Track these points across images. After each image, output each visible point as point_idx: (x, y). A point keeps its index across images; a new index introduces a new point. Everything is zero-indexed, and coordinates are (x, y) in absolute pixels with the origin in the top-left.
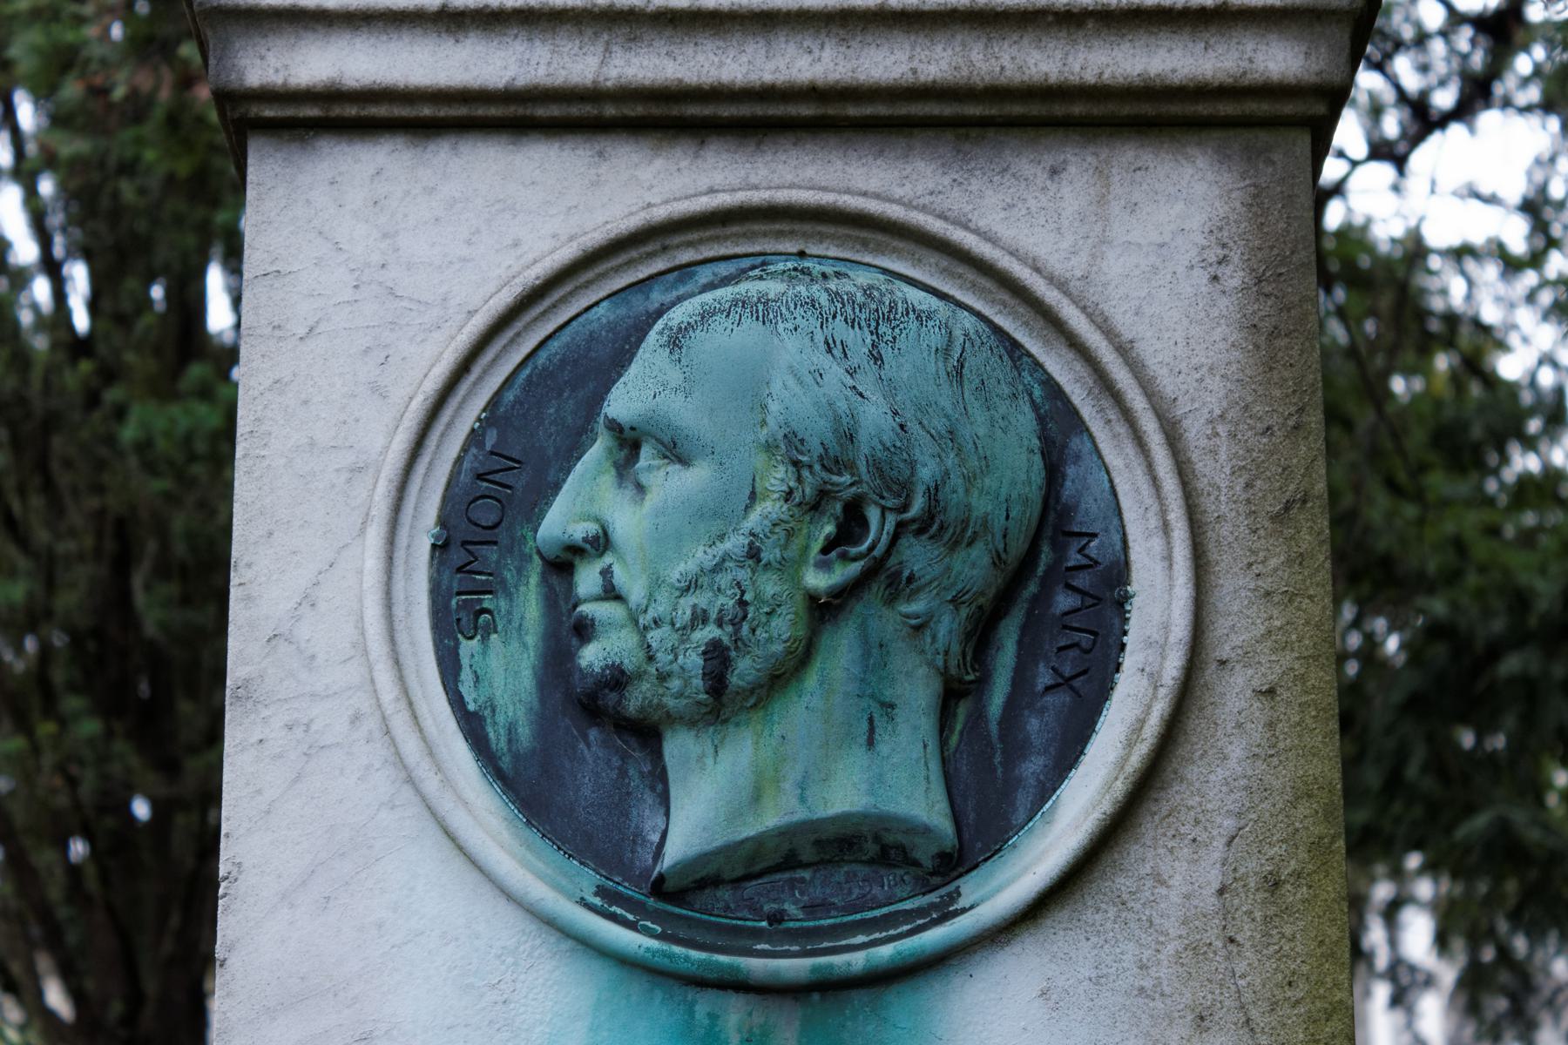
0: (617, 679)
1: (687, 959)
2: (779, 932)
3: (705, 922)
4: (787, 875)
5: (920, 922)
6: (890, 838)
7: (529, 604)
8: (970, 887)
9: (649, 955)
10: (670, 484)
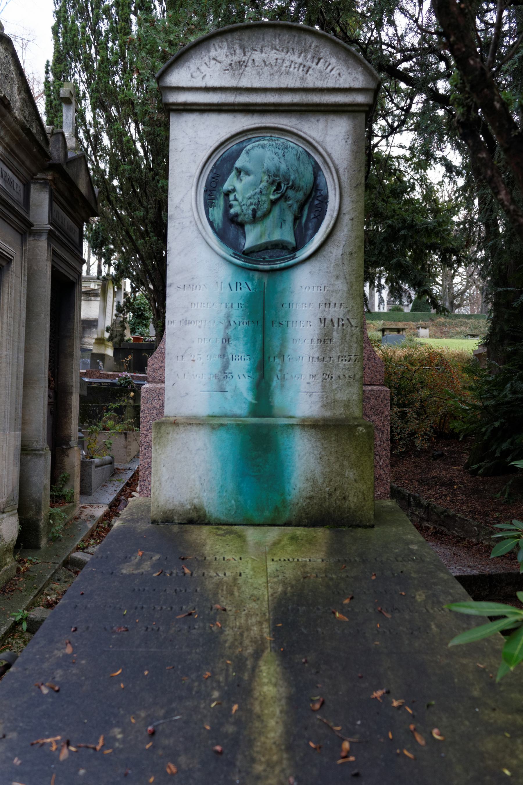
0: (237, 215)
2: (265, 261)
7: (221, 202)
8: (298, 253)
10: (246, 179)
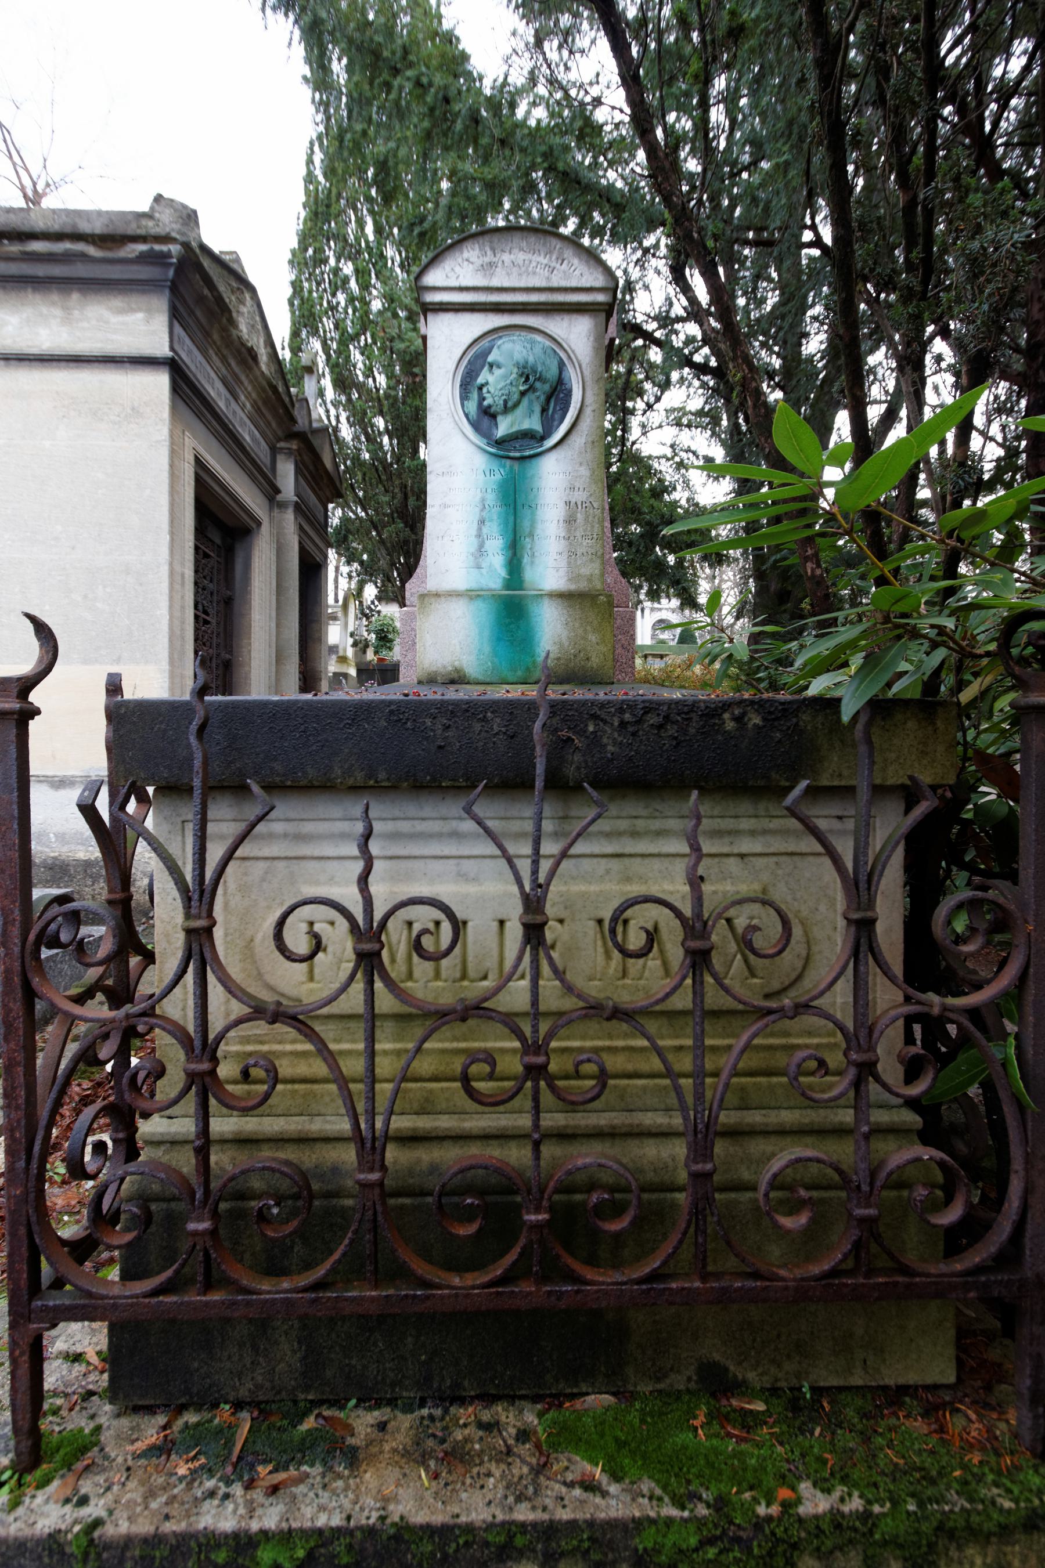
0: (490, 407)
2: (515, 449)
7: (475, 395)
10: (498, 372)
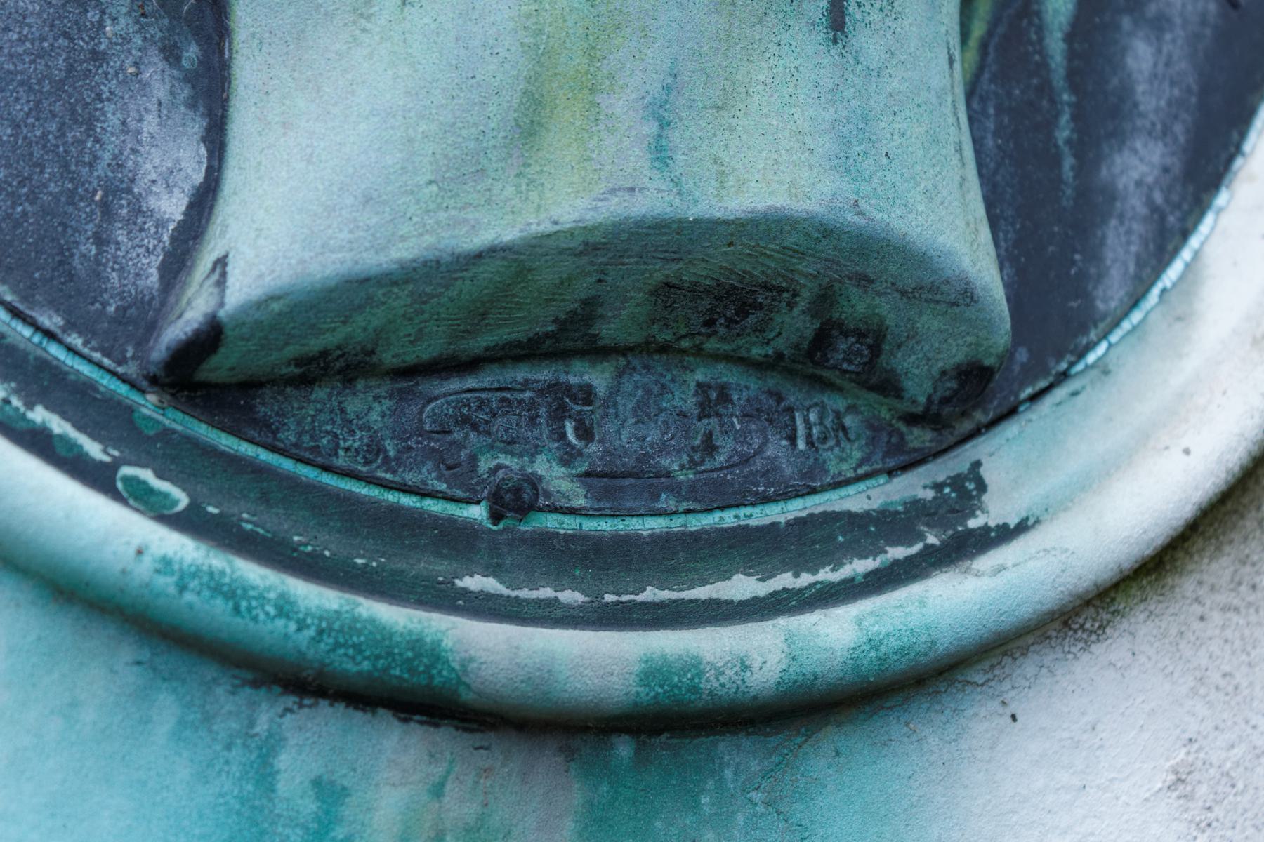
1: (285, 607)
3: (310, 488)
4: (544, 374)
5: (898, 552)
6: (857, 306)
8: (1013, 468)
9: (166, 583)
